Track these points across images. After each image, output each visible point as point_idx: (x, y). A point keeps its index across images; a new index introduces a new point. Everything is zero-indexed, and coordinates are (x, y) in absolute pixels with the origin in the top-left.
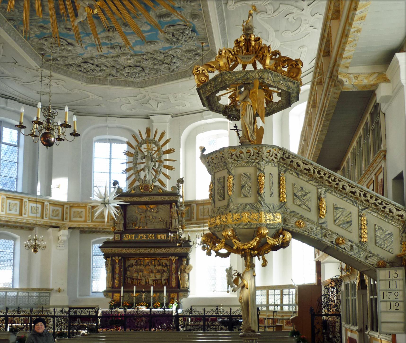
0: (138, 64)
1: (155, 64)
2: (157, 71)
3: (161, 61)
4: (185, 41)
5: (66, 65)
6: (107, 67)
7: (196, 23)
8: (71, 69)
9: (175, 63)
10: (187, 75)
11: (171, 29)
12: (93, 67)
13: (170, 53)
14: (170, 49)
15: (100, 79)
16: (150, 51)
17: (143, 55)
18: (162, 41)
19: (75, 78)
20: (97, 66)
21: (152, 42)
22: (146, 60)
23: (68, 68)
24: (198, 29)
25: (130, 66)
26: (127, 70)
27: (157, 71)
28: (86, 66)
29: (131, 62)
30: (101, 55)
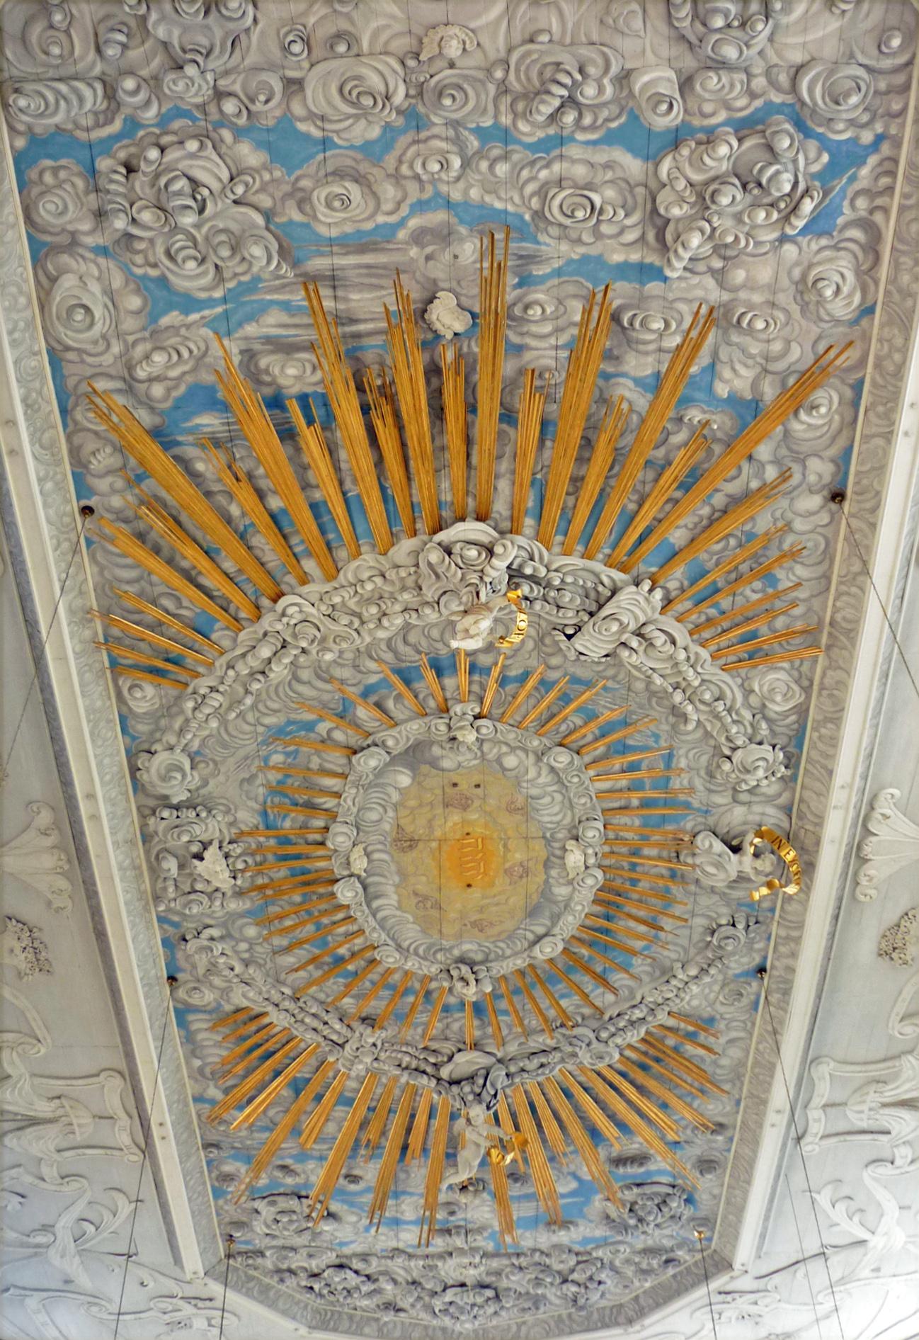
0: (488, 1280)
1: (538, 1282)
2: (537, 1301)
3: (559, 1273)
4: (657, 1225)
5: (279, 1271)
6: (395, 1282)
7: (705, 1185)
8: (291, 1281)
9: (600, 1283)
10: (621, 1319)
11: (629, 1195)
12: (353, 1280)
13: (600, 1253)
14: (604, 1242)
15: (351, 1318)
16: (544, 1247)
17: (518, 1255)
18: (591, 1221)
19: (285, 1313)
20: (368, 1277)
21: (565, 1224)
22: (521, 1268)
23: (282, 1280)
24: (703, 1197)
25: (463, 1285)
26: (449, 1296)
27: (537, 1301)
28: (337, 1278)
29: (471, 1275)
30: (397, 1249)
